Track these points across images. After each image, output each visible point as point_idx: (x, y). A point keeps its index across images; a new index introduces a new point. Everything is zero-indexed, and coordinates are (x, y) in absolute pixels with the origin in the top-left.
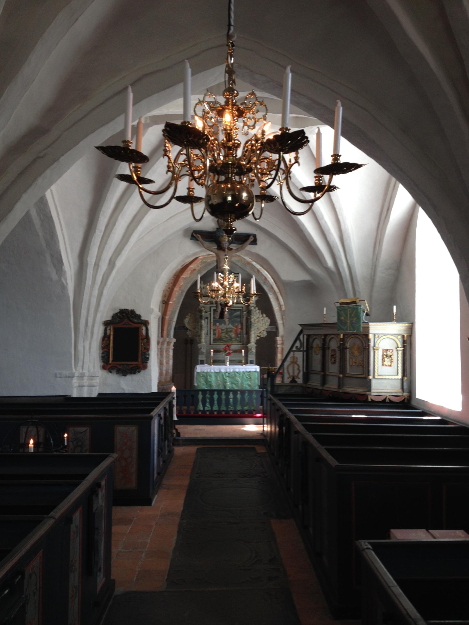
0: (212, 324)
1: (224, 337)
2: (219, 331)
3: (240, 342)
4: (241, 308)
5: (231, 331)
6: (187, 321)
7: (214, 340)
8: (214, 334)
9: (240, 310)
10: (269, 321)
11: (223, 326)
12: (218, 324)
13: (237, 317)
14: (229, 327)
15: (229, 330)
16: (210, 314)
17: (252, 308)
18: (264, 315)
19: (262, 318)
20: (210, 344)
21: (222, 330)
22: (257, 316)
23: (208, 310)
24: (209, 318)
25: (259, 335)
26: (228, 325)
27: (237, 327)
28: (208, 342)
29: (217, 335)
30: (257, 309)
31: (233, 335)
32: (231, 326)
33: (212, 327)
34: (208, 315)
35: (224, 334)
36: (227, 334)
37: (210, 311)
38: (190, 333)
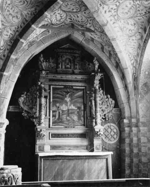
0: (51, 104)
1: (65, 120)
2: (59, 113)
3: (84, 126)
4: (84, 88)
5: (72, 113)
6: (21, 100)
7: (53, 123)
8: (54, 116)
9: (83, 89)
10: (114, 102)
11: (64, 107)
12: (58, 105)
13: (79, 97)
14: (70, 108)
15: (70, 111)
16: (50, 93)
17: (97, 87)
18: (109, 96)
19: (107, 100)
20: (49, 127)
21: (63, 111)
22: (102, 97)
23: (47, 88)
24: (48, 98)
25: (104, 117)
26: (70, 105)
27: (79, 108)
28: (48, 126)
29: (57, 117)
30: (101, 89)
31: (75, 118)
32: (72, 107)
33: (51, 108)
34: (47, 94)
35: (65, 116)
36: (68, 116)
37: (50, 89)
38: (26, 115)
